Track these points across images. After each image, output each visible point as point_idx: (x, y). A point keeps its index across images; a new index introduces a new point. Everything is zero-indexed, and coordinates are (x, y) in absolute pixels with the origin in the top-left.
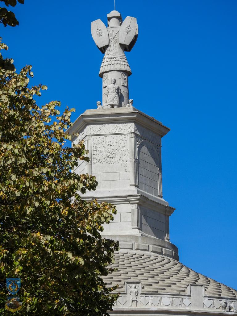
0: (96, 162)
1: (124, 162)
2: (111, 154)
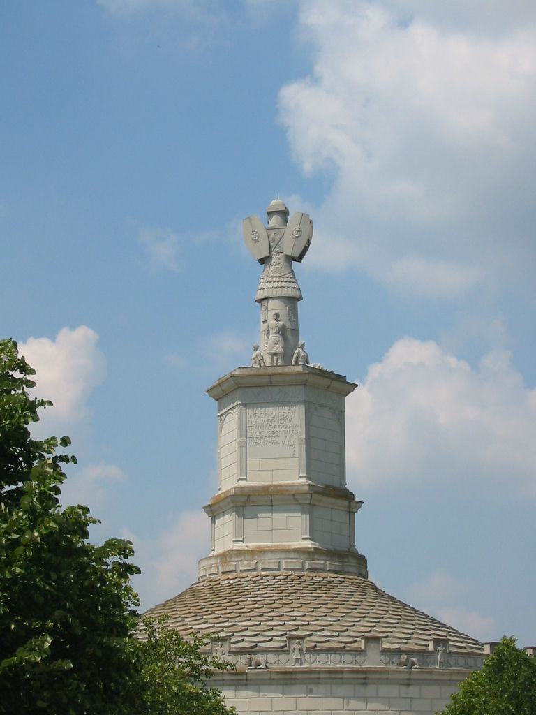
1: (292, 444)
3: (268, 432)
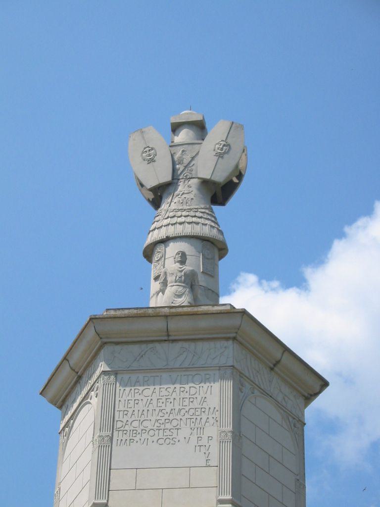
0: (123, 442)
1: (204, 441)
2: (167, 421)
3: (157, 421)
